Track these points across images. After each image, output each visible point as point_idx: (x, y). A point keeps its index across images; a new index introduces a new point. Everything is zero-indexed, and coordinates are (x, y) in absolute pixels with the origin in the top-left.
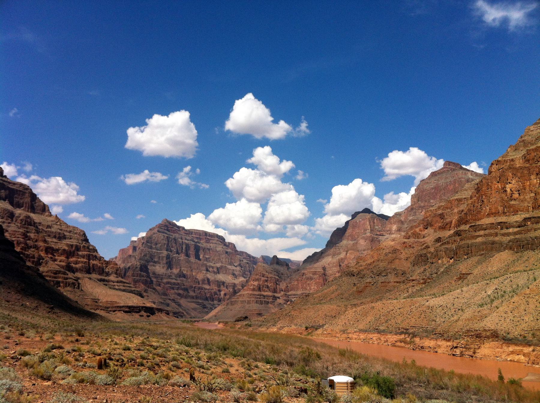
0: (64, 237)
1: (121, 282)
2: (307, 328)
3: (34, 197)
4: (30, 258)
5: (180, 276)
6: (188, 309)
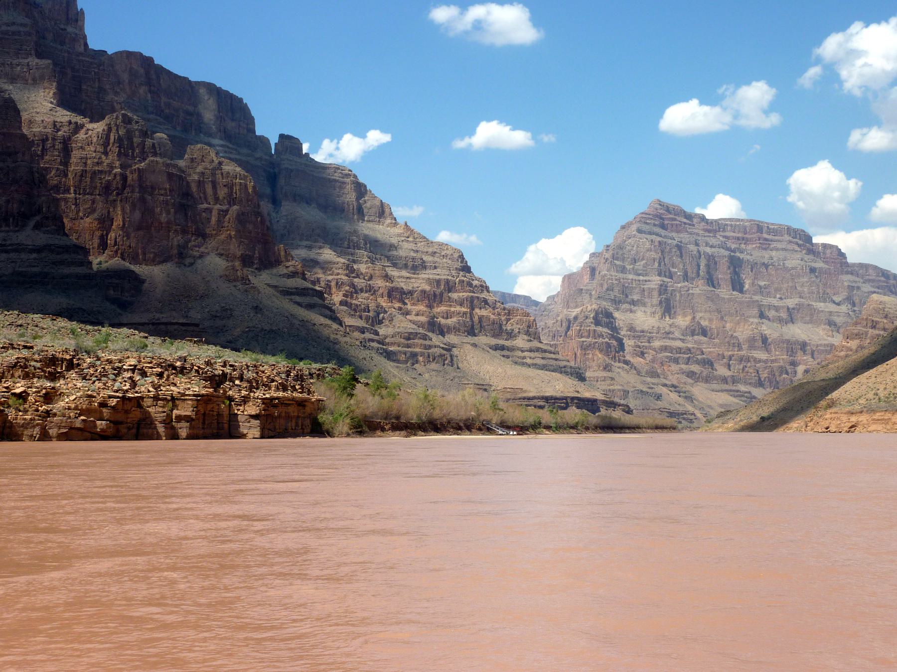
0: (423, 266)
1: (538, 350)
5: (693, 334)
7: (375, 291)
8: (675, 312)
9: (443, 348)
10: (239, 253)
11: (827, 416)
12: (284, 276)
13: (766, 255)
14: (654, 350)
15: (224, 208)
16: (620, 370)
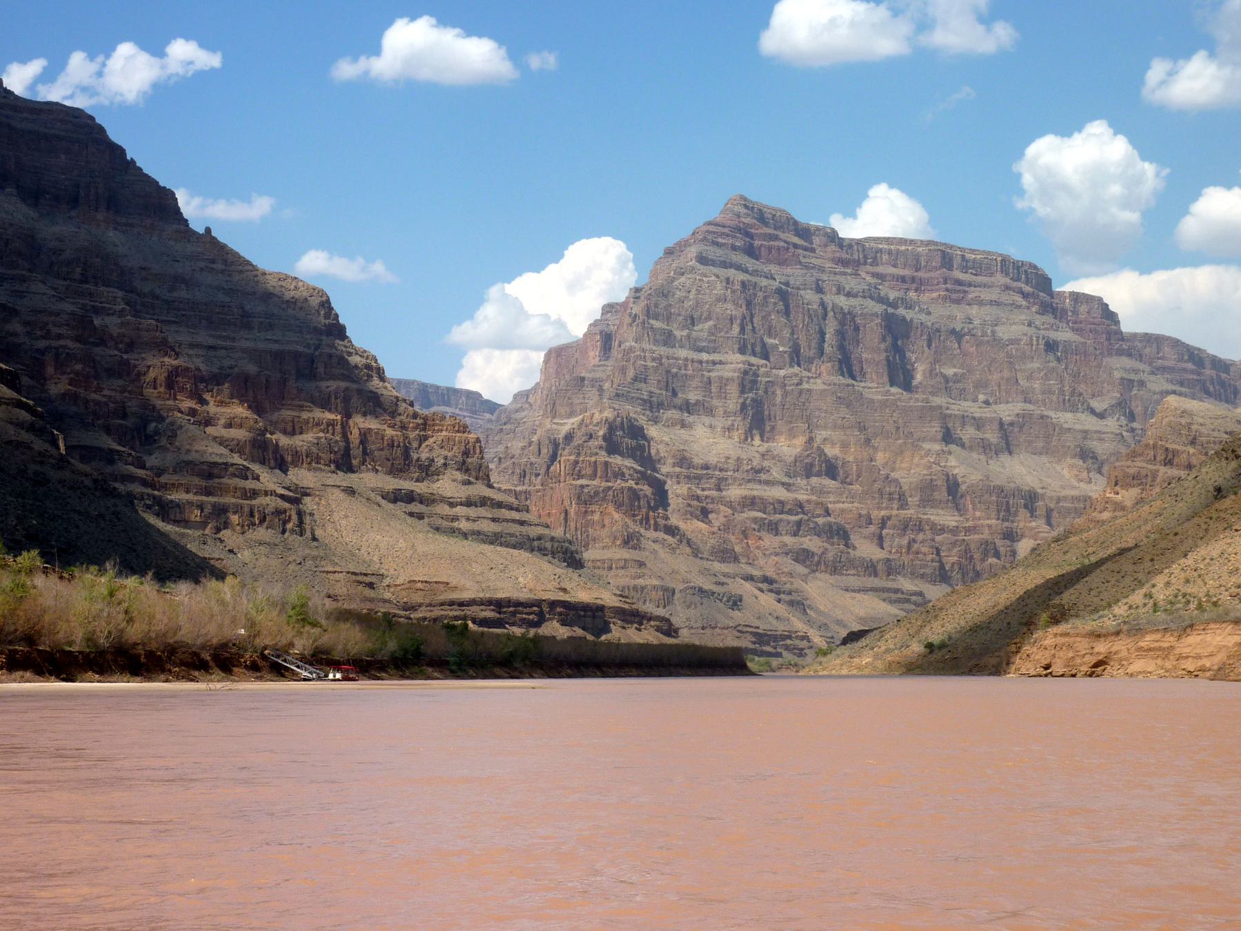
1: (484, 502)
5: (808, 472)
8: (773, 428)
9: (282, 497)
11: (1046, 642)
13: (959, 312)
14: (730, 505)
16: (656, 547)
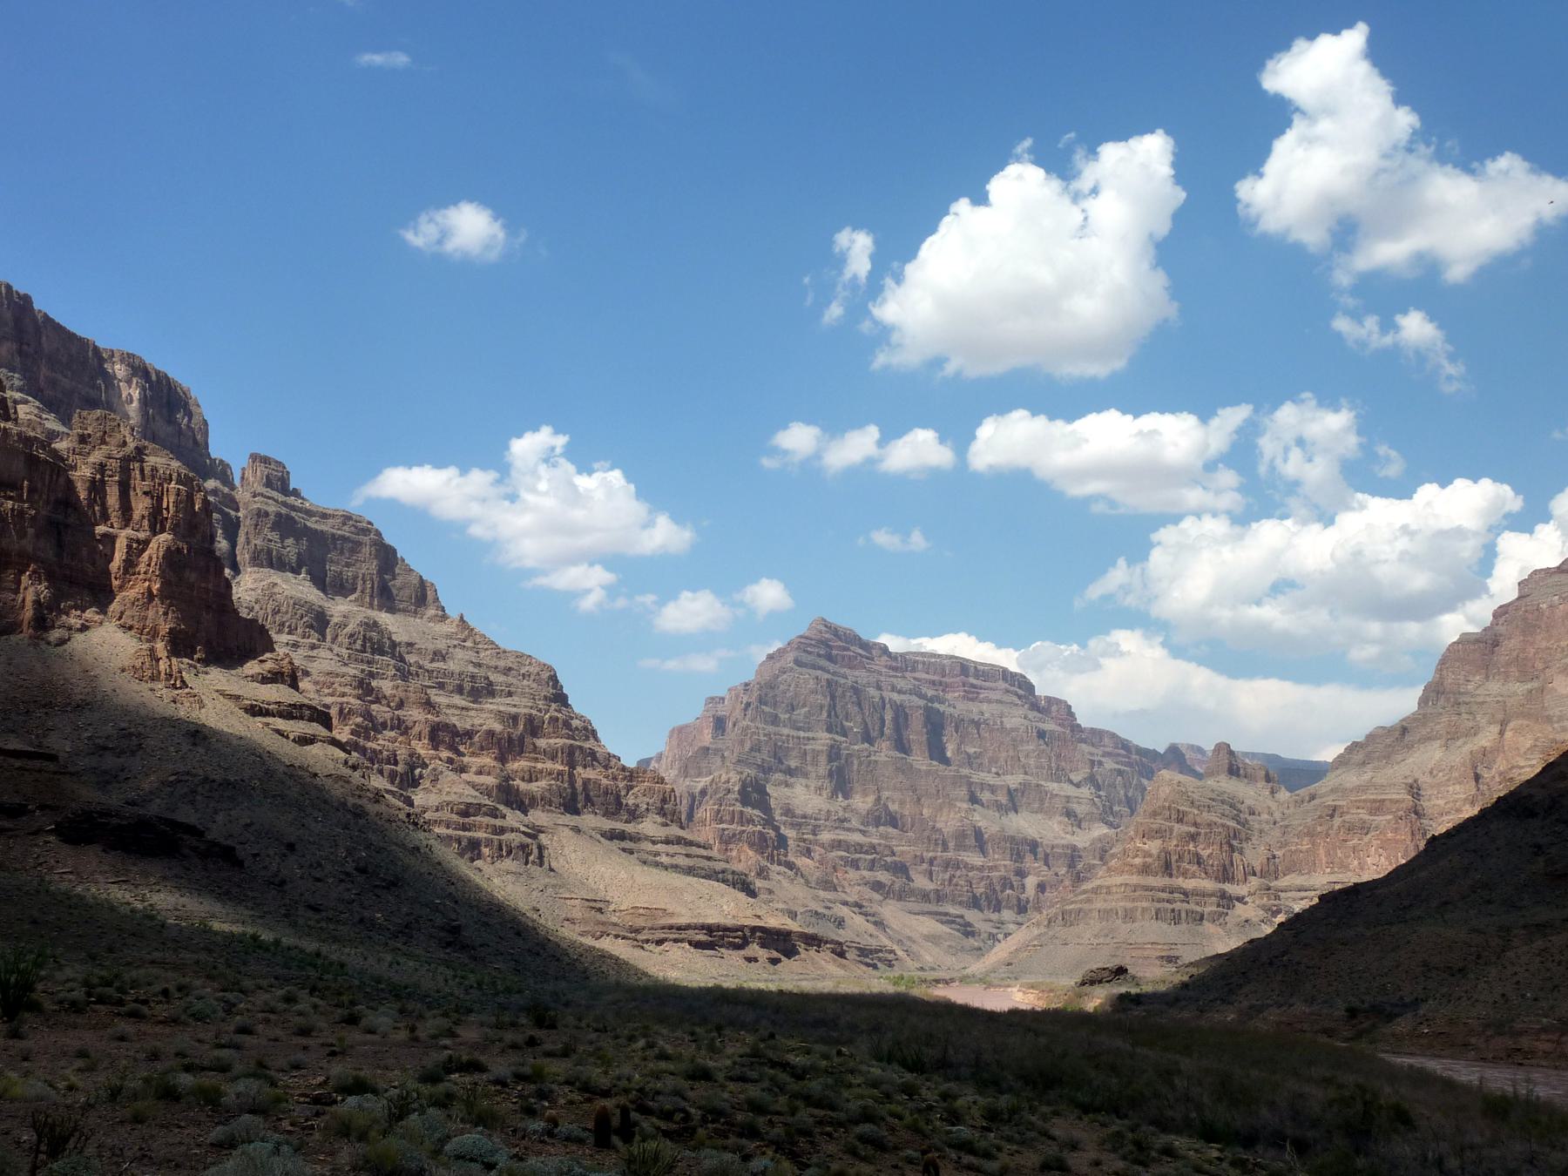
0: (490, 691)
1: (679, 841)
2: (1352, 1013)
3: (387, 558)
4: (380, 762)
5: (878, 823)
6: (909, 938)
7: (407, 728)
10: (164, 628)
12: (253, 678)
13: (974, 708)
14: (822, 846)
15: (142, 535)
